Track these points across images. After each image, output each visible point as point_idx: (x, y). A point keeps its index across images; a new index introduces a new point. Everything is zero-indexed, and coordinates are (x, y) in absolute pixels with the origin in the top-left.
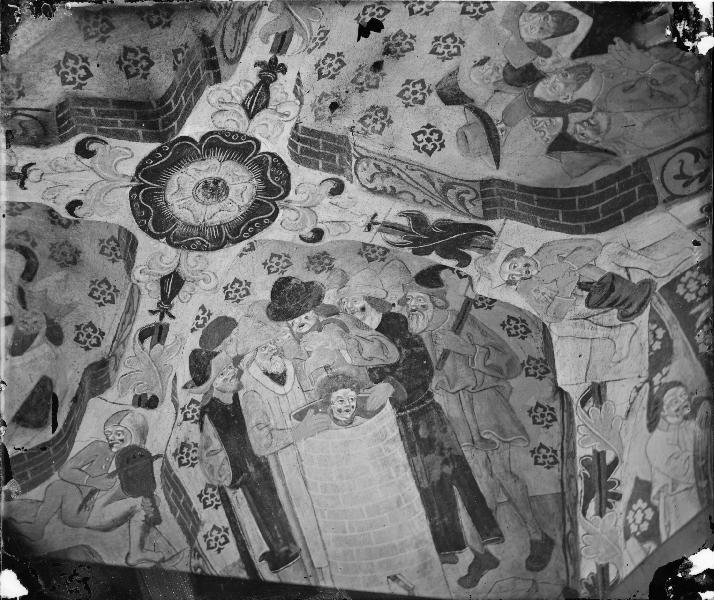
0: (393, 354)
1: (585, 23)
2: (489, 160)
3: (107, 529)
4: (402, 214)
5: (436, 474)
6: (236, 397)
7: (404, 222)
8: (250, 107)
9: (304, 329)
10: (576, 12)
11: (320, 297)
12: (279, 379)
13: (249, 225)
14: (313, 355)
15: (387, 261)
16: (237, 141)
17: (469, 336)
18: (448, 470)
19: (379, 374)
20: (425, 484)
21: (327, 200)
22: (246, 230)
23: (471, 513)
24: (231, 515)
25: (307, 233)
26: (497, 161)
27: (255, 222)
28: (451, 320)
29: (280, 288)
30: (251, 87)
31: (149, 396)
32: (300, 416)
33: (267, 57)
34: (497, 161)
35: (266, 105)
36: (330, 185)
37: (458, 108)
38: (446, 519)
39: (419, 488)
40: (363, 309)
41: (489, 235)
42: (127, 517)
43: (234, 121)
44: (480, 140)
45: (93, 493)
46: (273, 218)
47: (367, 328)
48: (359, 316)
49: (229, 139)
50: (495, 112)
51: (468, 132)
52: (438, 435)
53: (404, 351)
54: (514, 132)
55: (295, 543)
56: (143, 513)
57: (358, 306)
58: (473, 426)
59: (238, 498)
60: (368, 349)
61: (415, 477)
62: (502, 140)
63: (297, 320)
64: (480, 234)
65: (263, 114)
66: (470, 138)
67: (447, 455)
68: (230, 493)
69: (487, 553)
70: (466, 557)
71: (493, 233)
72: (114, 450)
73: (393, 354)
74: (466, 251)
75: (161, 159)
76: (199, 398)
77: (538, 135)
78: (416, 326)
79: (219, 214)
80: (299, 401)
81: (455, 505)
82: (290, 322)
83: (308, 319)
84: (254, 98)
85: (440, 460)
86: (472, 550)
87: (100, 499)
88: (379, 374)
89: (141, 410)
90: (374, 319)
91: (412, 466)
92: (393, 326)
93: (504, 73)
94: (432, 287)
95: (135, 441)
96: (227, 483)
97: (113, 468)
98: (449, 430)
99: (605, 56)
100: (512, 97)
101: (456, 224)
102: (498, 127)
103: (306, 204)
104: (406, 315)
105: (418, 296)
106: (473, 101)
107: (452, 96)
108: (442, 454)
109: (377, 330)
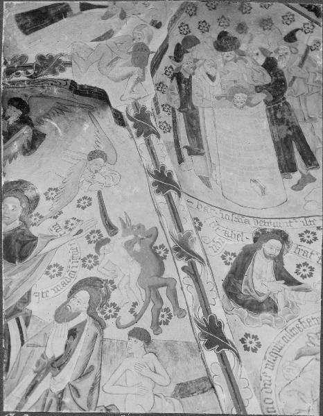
0: (268, 79)
3: (117, 81)
5: (283, 136)
6: (191, 77)
9: (229, 59)
11: (238, 46)
12: (212, 78)
14: (230, 74)
17: (307, 68)
18: (290, 133)
19: (259, 89)
20: (277, 139)
23: (301, 154)
24: (174, 122)
28: (299, 60)
29: (223, 35)
31: (158, 22)
32: (218, 98)
38: (287, 157)
39: (274, 141)
40: (257, 54)
42: (129, 76)
45: (117, 58)
47: (258, 65)
48: (255, 57)
52: (287, 117)
53: (274, 78)
55: (203, 149)
56: (137, 75)
57: (255, 52)
58: (305, 112)
59: (180, 117)
60: (257, 76)
61: (273, 137)
63: (226, 53)
67: (290, 126)
68: (177, 112)
69: (309, 175)
70: (296, 176)
72: (134, 42)
73: (268, 79)
76: (174, 67)
78: (281, 65)
80: (219, 92)
81: (293, 149)
82: (223, 53)
83: (230, 55)
85: (287, 127)
86: (301, 172)
87: (120, 63)
88: (259, 89)
89: (152, 28)
90: (262, 60)
91: (272, 131)
92: (270, 65)
94: (292, 42)
95: (145, 41)
96: (177, 106)
97: (131, 50)
98: (293, 115)
104: (277, 59)
105: (285, 47)
108: (287, 125)
109: (262, 66)
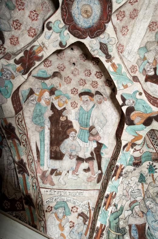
1: (59, 109)
2: (36, 75)
4: (42, 56)
7: (40, 55)
8: (104, 46)
10: (62, 108)
13: (66, 11)
15: (11, 27)
16: (96, 33)
21: (59, 39)
22: (65, 8)
25: (50, 25)
26: (34, 77)
27: (66, 14)
30: (109, 51)
33: (114, 61)
34: (34, 77)
35: (100, 49)
36: (64, 44)
37: (52, 74)
41: (23, 73)
43: (103, 38)
44: (41, 75)
46: (64, 20)
49: (99, 32)
50: (47, 82)
51: (45, 73)
54: (40, 84)
62: (39, 80)
64: (24, 72)
65: (99, 47)
66: (43, 73)
71: (23, 74)
74: (20, 65)
75: (108, 9)
77: (37, 88)
79: (77, 6)
84: (105, 49)
93: (55, 88)
99: (50, 109)
100: (48, 87)
101: (31, 67)
102: (43, 81)
103: (62, 33)
106: (52, 78)
107: (55, 74)
